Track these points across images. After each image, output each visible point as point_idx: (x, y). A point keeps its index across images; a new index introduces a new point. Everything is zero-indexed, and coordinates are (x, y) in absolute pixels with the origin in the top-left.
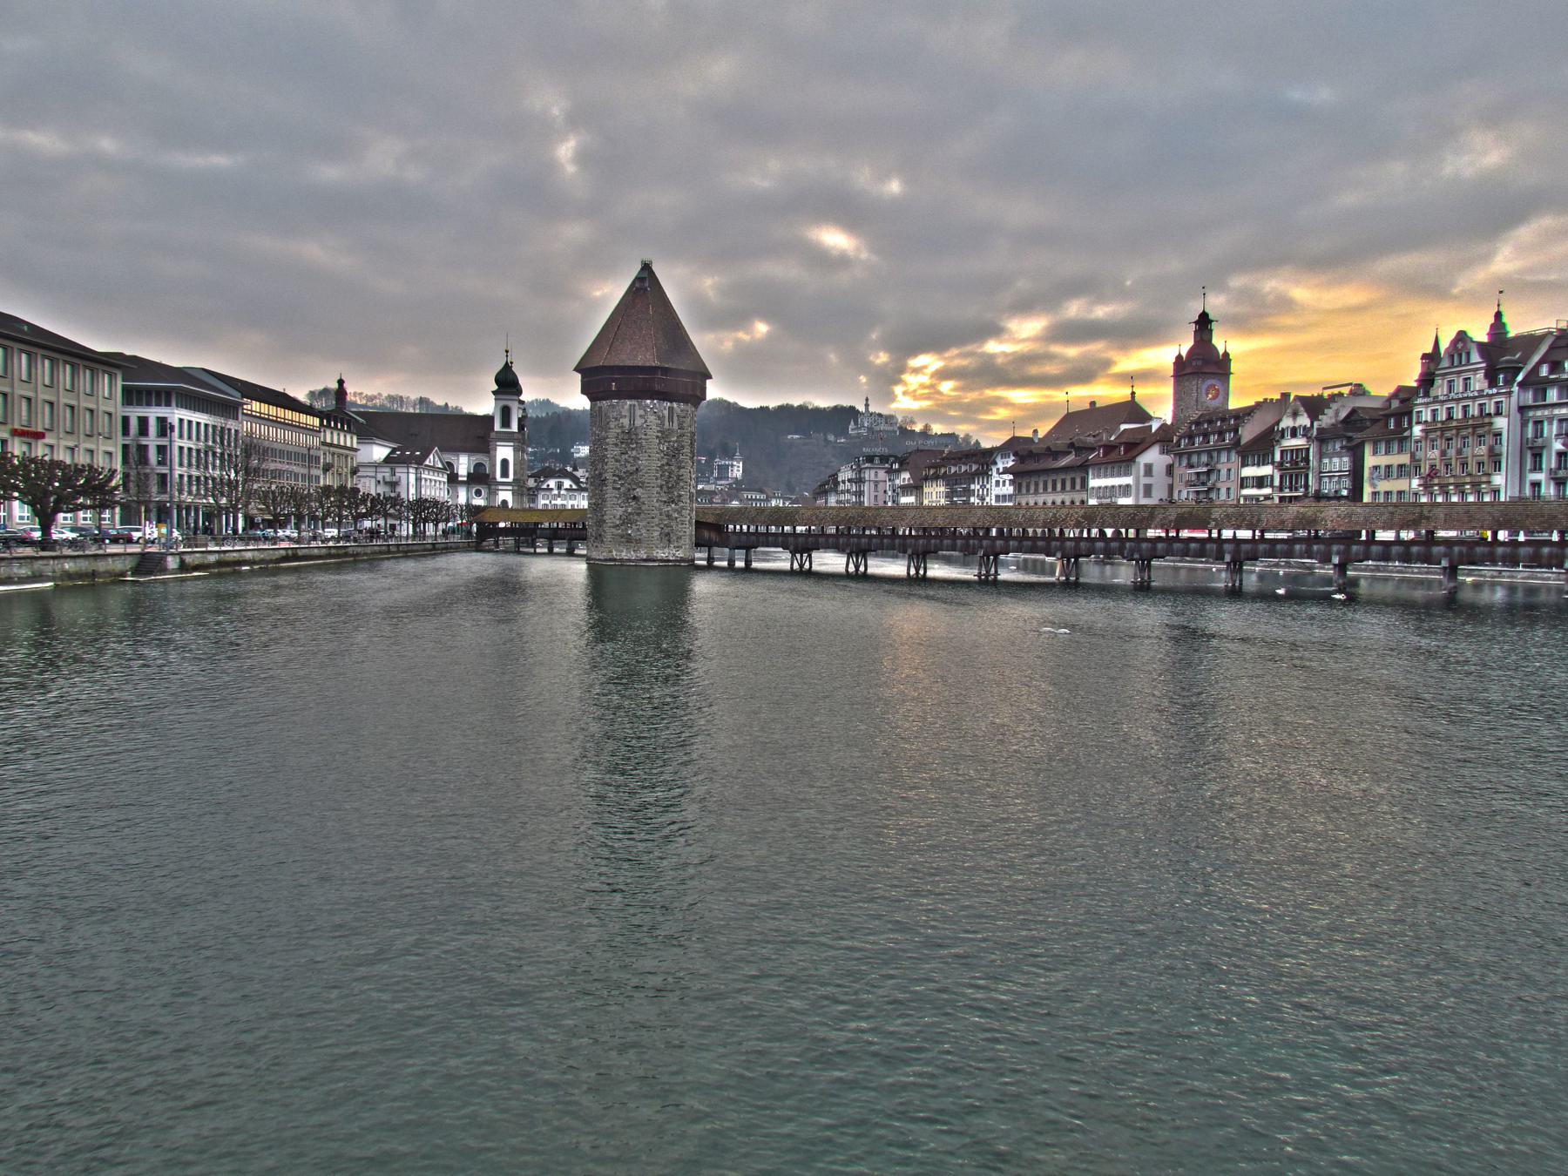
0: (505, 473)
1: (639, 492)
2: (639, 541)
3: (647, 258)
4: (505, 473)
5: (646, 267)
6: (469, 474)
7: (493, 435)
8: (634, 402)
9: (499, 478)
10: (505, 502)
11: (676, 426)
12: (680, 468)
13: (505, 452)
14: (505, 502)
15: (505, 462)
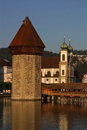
0: (63, 74)
1: (20, 80)
2: (20, 94)
3: (27, 16)
4: (63, 74)
5: (27, 18)
6: (54, 75)
7: (60, 62)
8: (19, 55)
9: (62, 75)
10: (63, 82)
11: (30, 61)
12: (32, 73)
13: (63, 67)
14: (63, 82)
15: (63, 71)
